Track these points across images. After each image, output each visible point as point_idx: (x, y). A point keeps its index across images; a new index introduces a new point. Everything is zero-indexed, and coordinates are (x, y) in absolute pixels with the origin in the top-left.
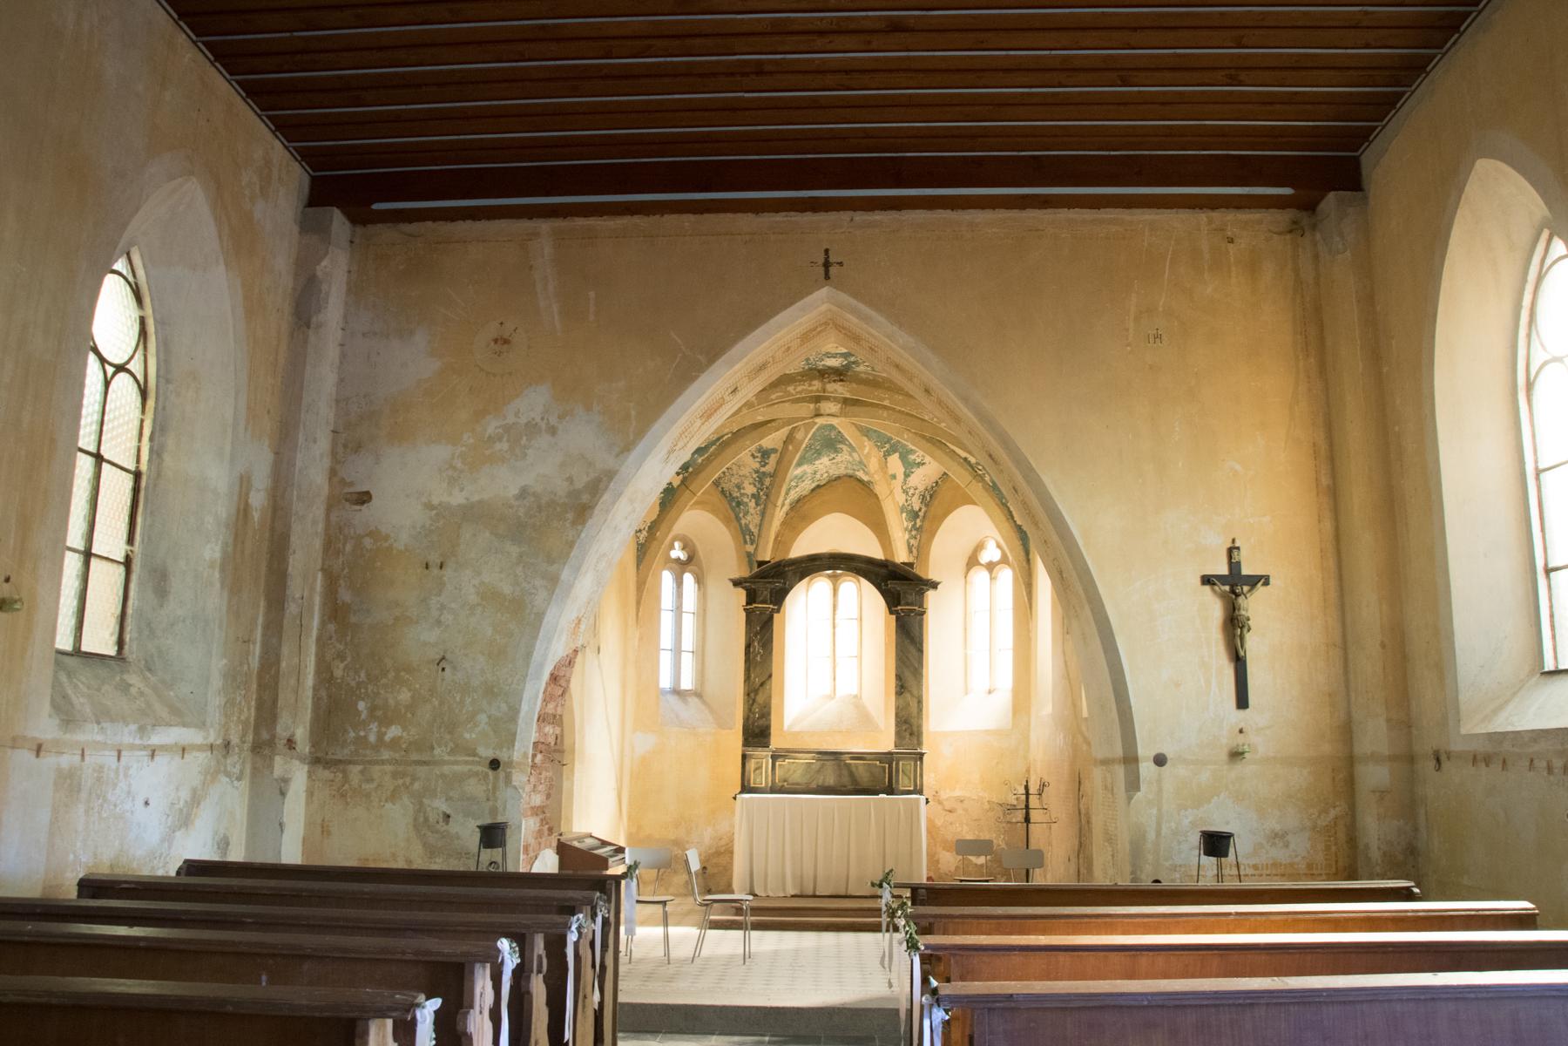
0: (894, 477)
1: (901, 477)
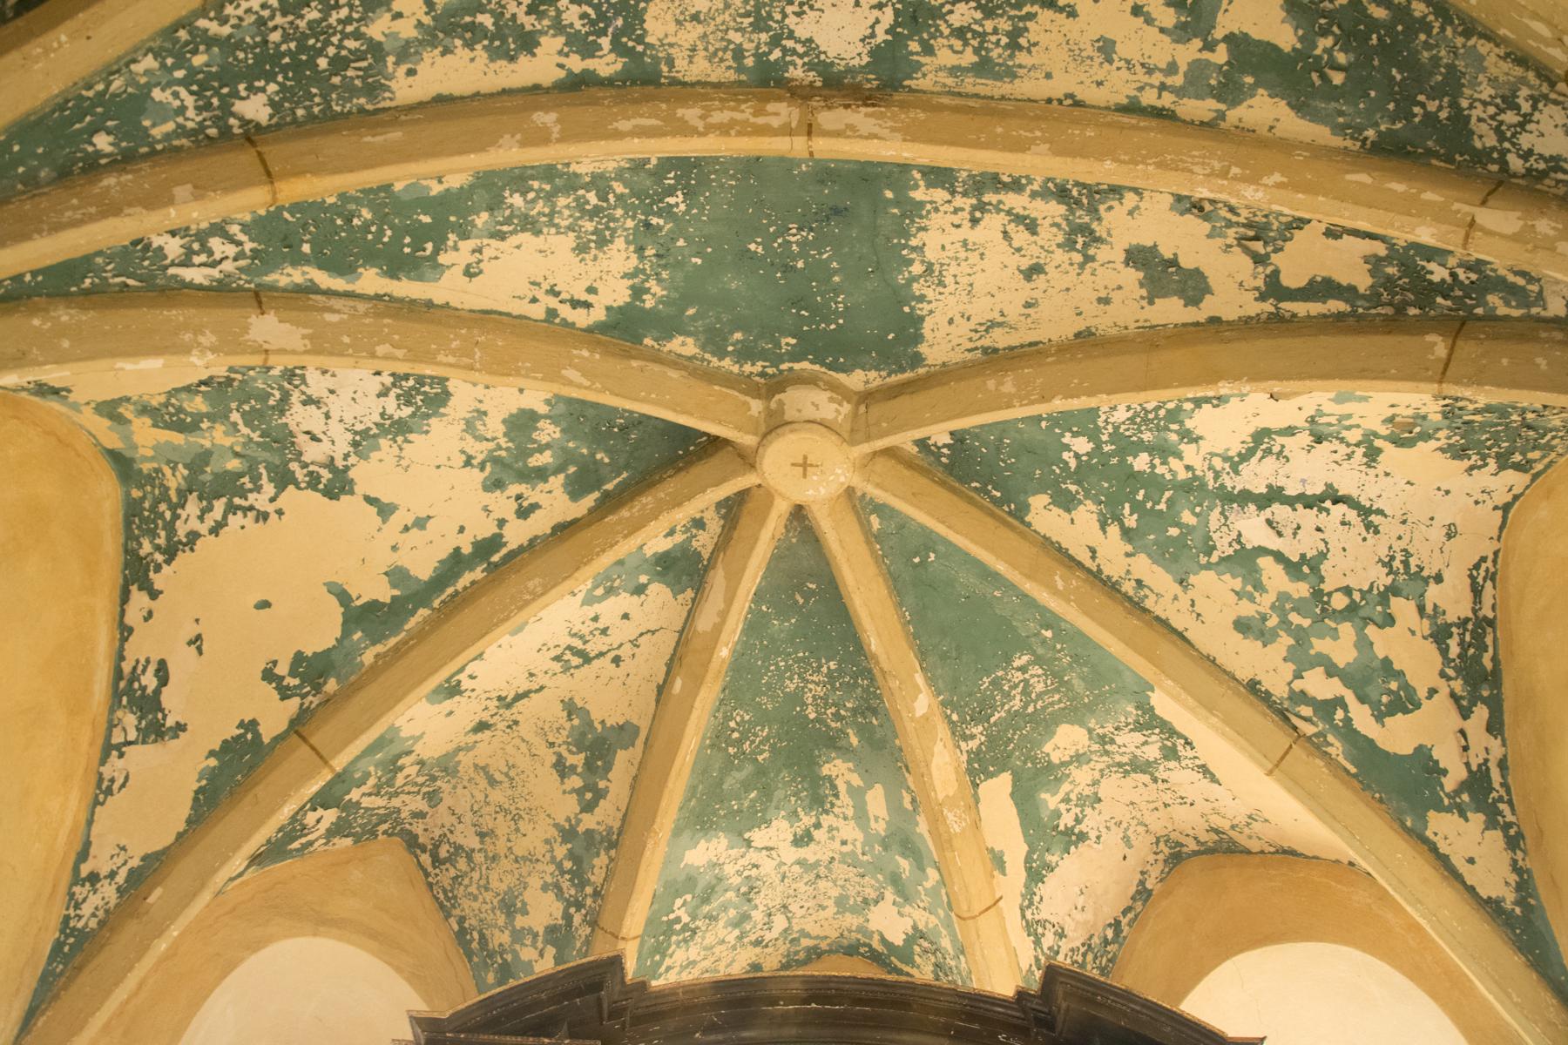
0: (998, 861)
1: (1017, 874)
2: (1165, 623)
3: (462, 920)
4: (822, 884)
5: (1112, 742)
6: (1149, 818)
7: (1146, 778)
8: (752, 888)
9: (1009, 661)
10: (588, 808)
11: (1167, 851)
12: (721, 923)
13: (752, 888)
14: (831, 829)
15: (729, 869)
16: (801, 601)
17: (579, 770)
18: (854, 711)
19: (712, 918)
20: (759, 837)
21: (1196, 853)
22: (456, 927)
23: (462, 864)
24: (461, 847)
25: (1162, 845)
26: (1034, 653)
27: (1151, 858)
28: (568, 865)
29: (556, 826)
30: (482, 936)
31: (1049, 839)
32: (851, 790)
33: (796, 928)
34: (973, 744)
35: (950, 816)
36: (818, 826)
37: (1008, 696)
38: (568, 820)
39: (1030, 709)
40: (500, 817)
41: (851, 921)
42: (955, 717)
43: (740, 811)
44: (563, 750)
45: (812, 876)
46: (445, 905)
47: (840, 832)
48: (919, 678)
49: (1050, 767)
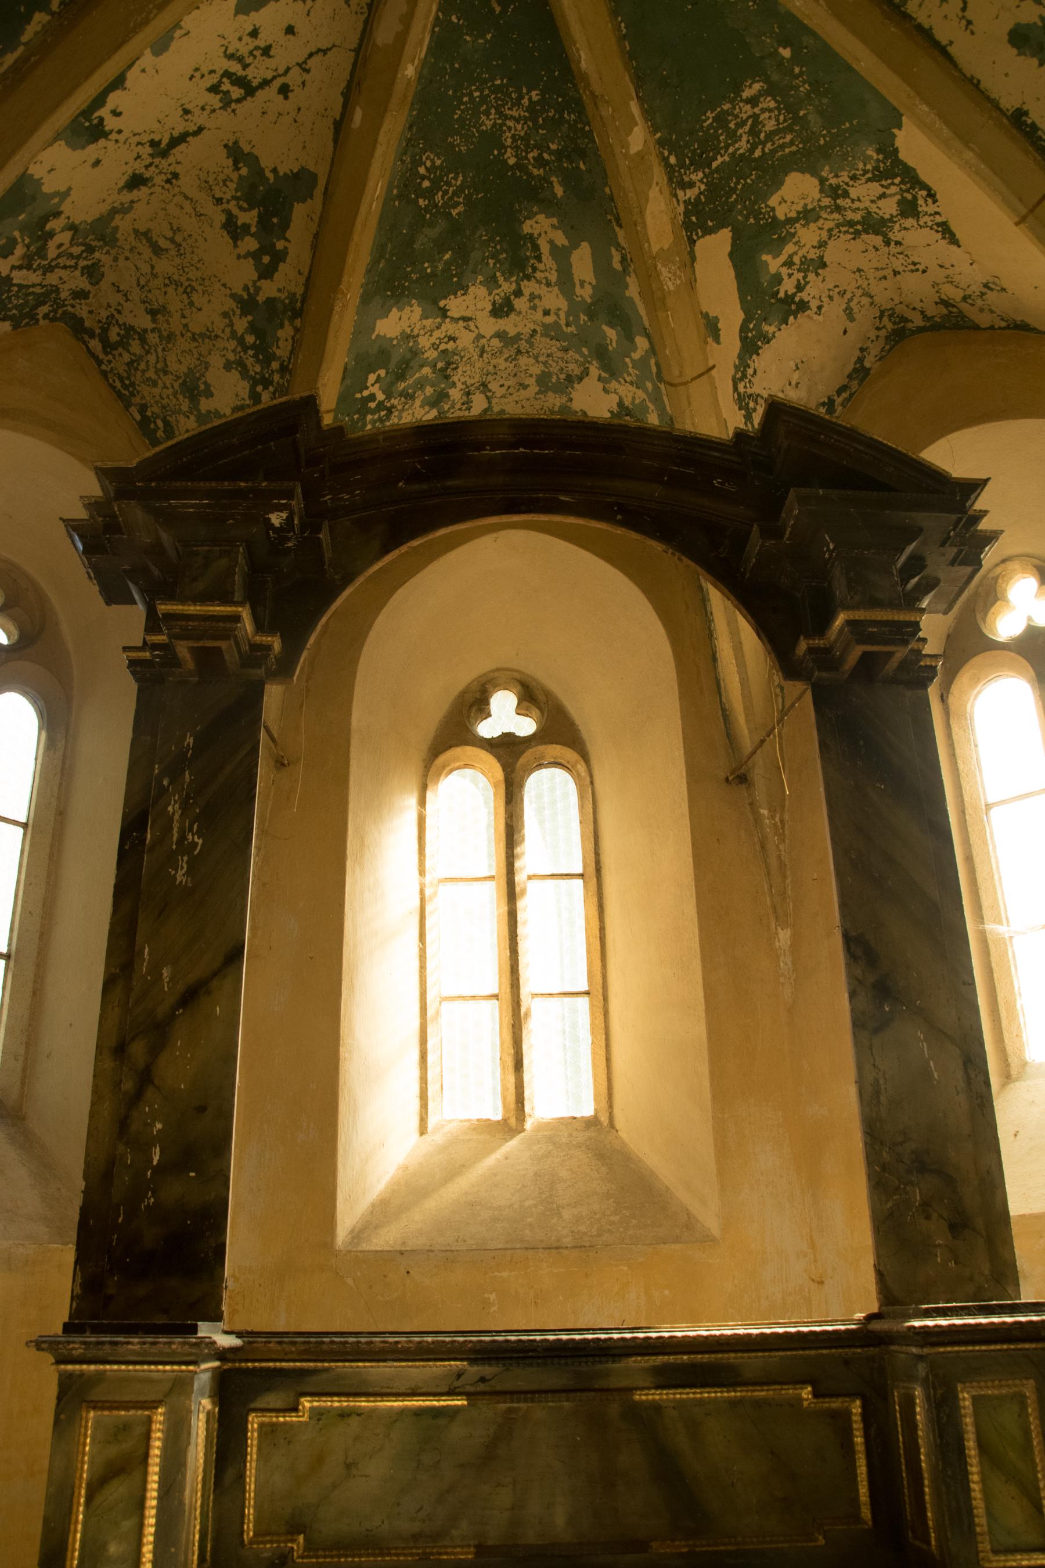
0: (712, 328)
2: (925, 34)
3: (143, 409)
4: (523, 360)
5: (846, 195)
6: (876, 289)
7: (878, 240)
8: (449, 364)
9: (738, 89)
10: (267, 273)
11: (890, 326)
12: (418, 402)
13: (449, 364)
14: (533, 297)
15: (424, 342)
16: (498, 9)
17: (253, 230)
18: (559, 153)
19: (408, 396)
20: (455, 305)
21: (921, 330)
22: (138, 417)
23: (136, 347)
24: (132, 328)
25: (885, 319)
26: (767, 80)
27: (872, 334)
28: (250, 339)
29: (233, 296)
30: (167, 423)
31: (767, 306)
32: (556, 251)
33: (496, 409)
34: (691, 194)
35: (664, 272)
36: (518, 293)
37: (733, 136)
38: (246, 288)
39: (758, 153)
40: (171, 290)
41: (554, 401)
42: (673, 160)
43: (433, 275)
44: (232, 206)
45: (513, 352)
46: (124, 394)
47: (544, 301)
48: (634, 108)
49: (775, 224)
